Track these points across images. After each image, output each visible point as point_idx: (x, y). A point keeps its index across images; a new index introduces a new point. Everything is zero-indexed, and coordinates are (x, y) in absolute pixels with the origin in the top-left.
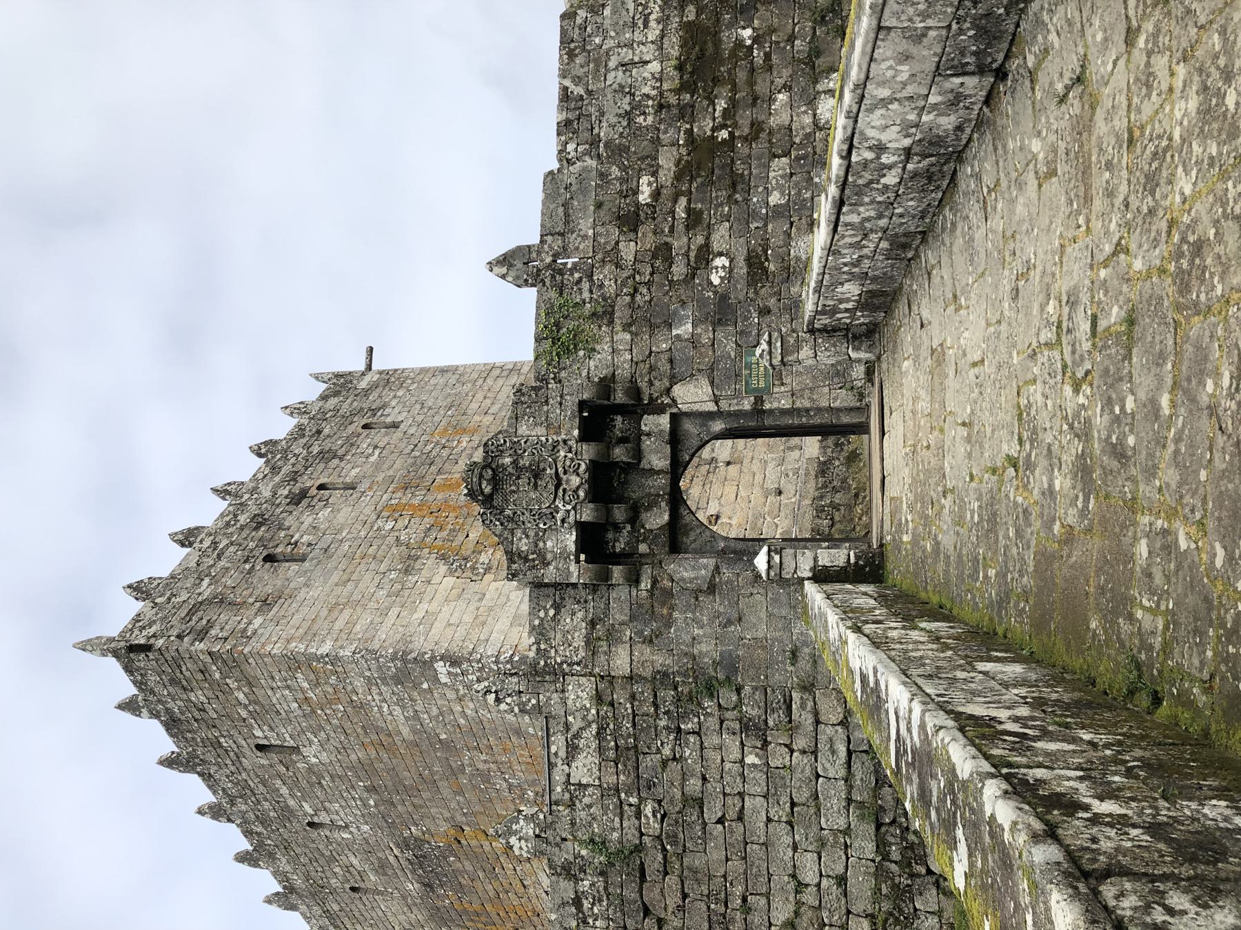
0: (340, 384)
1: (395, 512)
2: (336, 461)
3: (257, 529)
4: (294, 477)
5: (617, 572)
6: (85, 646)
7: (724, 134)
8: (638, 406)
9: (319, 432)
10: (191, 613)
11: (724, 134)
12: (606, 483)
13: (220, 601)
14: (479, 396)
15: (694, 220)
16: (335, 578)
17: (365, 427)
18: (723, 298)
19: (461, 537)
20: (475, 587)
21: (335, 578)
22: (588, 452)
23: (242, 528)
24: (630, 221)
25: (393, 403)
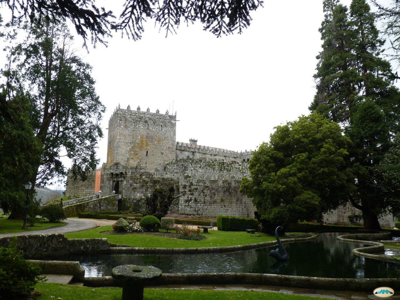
0: (173, 118)
1: (142, 137)
2: (153, 124)
3: (139, 118)
4: (150, 119)
5: (110, 176)
6: (119, 105)
7: (148, 185)
8: (124, 177)
9: (161, 119)
10: (124, 117)
11: (148, 185)
12: (117, 175)
13: (126, 120)
14: (167, 142)
15: (140, 182)
16: (130, 134)
17: (162, 126)
18: (132, 185)
19: (136, 148)
20: (128, 152)
21: (130, 134)
22: (119, 173)
23: (140, 116)
24: (141, 175)
25: (167, 128)
